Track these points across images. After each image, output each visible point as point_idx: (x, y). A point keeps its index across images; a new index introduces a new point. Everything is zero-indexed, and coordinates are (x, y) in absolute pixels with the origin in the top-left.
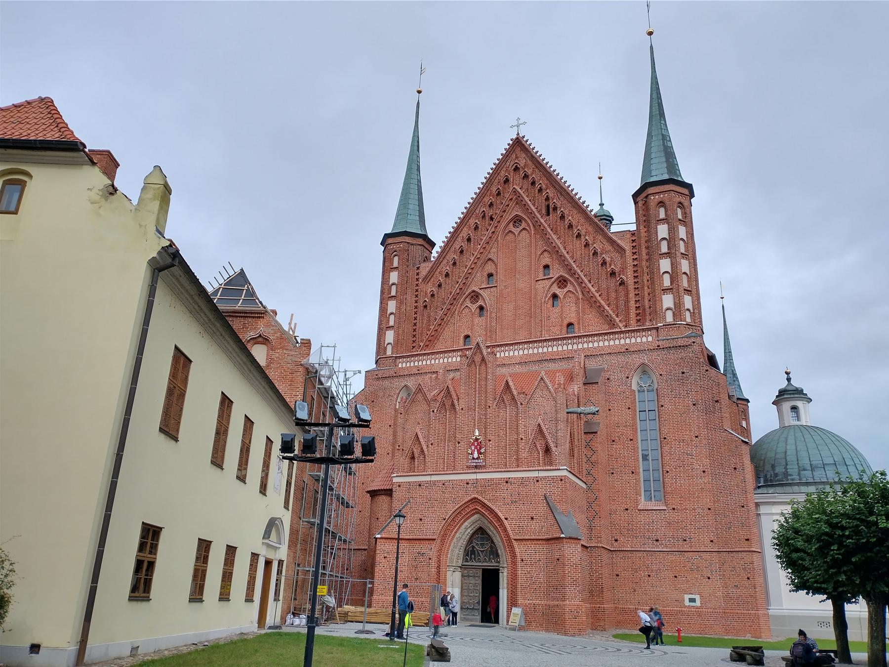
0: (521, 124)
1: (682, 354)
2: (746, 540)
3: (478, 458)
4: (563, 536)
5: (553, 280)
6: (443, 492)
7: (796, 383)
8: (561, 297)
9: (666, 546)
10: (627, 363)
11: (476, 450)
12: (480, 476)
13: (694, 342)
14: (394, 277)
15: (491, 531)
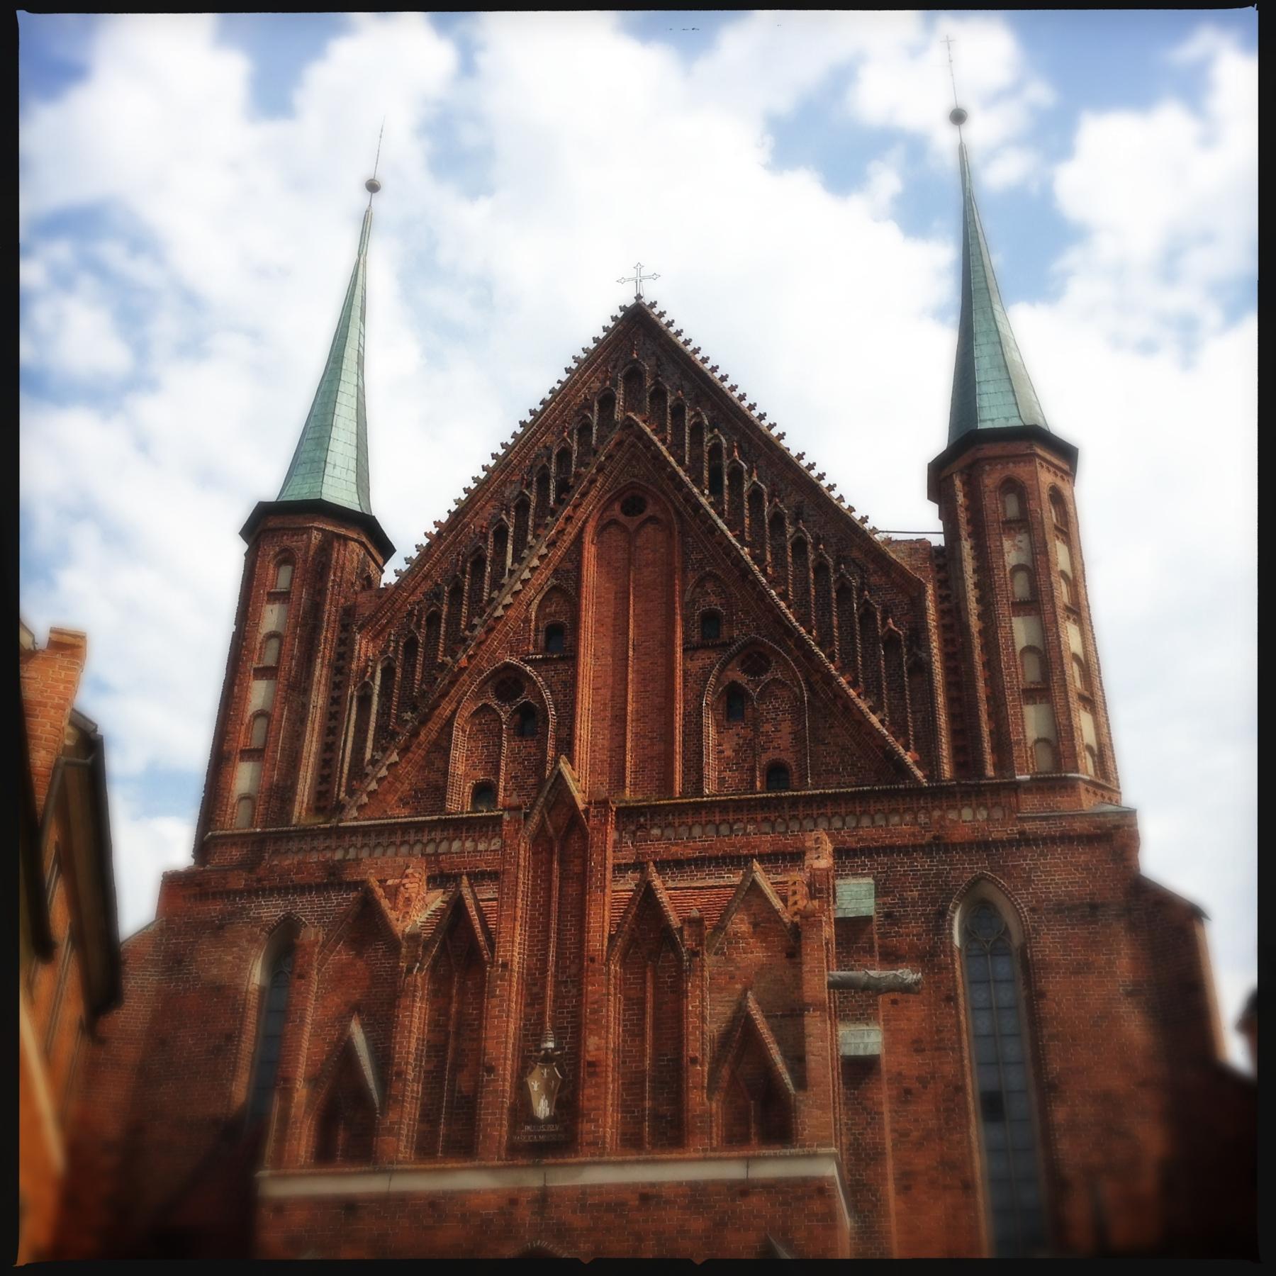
8: (755, 695)
14: (271, 618)
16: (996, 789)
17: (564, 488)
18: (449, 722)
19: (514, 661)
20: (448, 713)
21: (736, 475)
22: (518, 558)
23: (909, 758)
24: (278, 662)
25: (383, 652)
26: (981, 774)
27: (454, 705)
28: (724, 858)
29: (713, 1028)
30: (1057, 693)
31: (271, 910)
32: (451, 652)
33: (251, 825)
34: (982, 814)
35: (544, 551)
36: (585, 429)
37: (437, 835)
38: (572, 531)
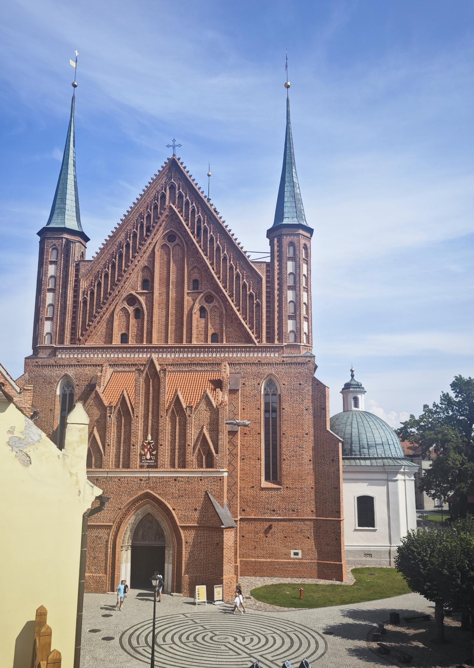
0: (177, 146)
1: (300, 369)
2: (337, 512)
3: (151, 459)
4: (223, 526)
6: (119, 486)
9: (280, 515)
10: (259, 373)
11: (149, 452)
13: (309, 361)
17: (148, 230)
18: (113, 312)
19: (133, 293)
20: (112, 309)
23: (253, 336)
24: (55, 287)
25: (91, 285)
26: (273, 342)
27: (114, 307)
28: (198, 364)
36: (156, 207)
38: (152, 247)
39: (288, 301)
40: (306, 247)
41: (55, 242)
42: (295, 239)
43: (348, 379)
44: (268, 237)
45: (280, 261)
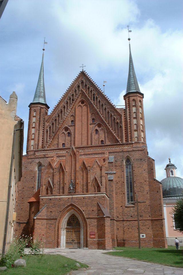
4: (105, 216)
5: (96, 124)
7: (172, 162)
12: (74, 196)
15: (77, 215)
16: (130, 144)
21: (97, 98)
22: (67, 111)
23: (119, 140)
29: (92, 179)
30: (138, 130)
31: (37, 161)
32: (58, 125)
33: (33, 149)
34: (128, 147)
35: (70, 110)
37: (58, 151)
39: (134, 124)
40: (140, 101)
41: (35, 108)
42: (135, 98)
43: (168, 163)
44: (125, 99)
45: (129, 107)
